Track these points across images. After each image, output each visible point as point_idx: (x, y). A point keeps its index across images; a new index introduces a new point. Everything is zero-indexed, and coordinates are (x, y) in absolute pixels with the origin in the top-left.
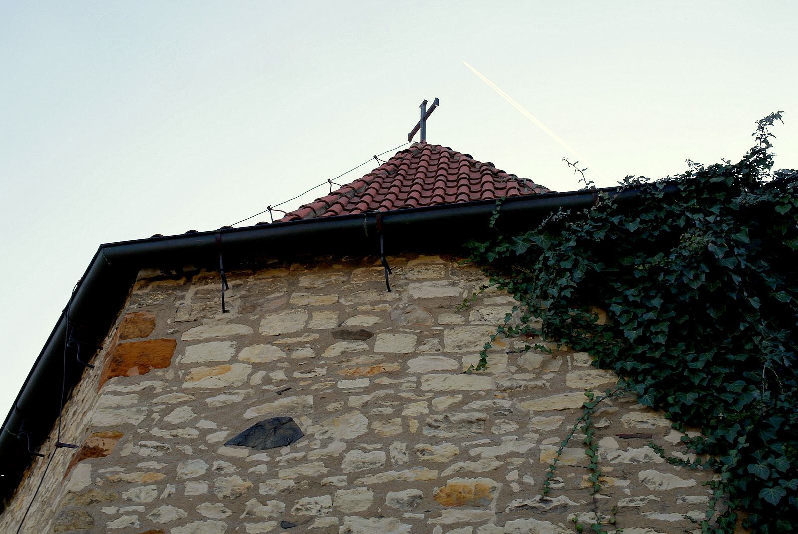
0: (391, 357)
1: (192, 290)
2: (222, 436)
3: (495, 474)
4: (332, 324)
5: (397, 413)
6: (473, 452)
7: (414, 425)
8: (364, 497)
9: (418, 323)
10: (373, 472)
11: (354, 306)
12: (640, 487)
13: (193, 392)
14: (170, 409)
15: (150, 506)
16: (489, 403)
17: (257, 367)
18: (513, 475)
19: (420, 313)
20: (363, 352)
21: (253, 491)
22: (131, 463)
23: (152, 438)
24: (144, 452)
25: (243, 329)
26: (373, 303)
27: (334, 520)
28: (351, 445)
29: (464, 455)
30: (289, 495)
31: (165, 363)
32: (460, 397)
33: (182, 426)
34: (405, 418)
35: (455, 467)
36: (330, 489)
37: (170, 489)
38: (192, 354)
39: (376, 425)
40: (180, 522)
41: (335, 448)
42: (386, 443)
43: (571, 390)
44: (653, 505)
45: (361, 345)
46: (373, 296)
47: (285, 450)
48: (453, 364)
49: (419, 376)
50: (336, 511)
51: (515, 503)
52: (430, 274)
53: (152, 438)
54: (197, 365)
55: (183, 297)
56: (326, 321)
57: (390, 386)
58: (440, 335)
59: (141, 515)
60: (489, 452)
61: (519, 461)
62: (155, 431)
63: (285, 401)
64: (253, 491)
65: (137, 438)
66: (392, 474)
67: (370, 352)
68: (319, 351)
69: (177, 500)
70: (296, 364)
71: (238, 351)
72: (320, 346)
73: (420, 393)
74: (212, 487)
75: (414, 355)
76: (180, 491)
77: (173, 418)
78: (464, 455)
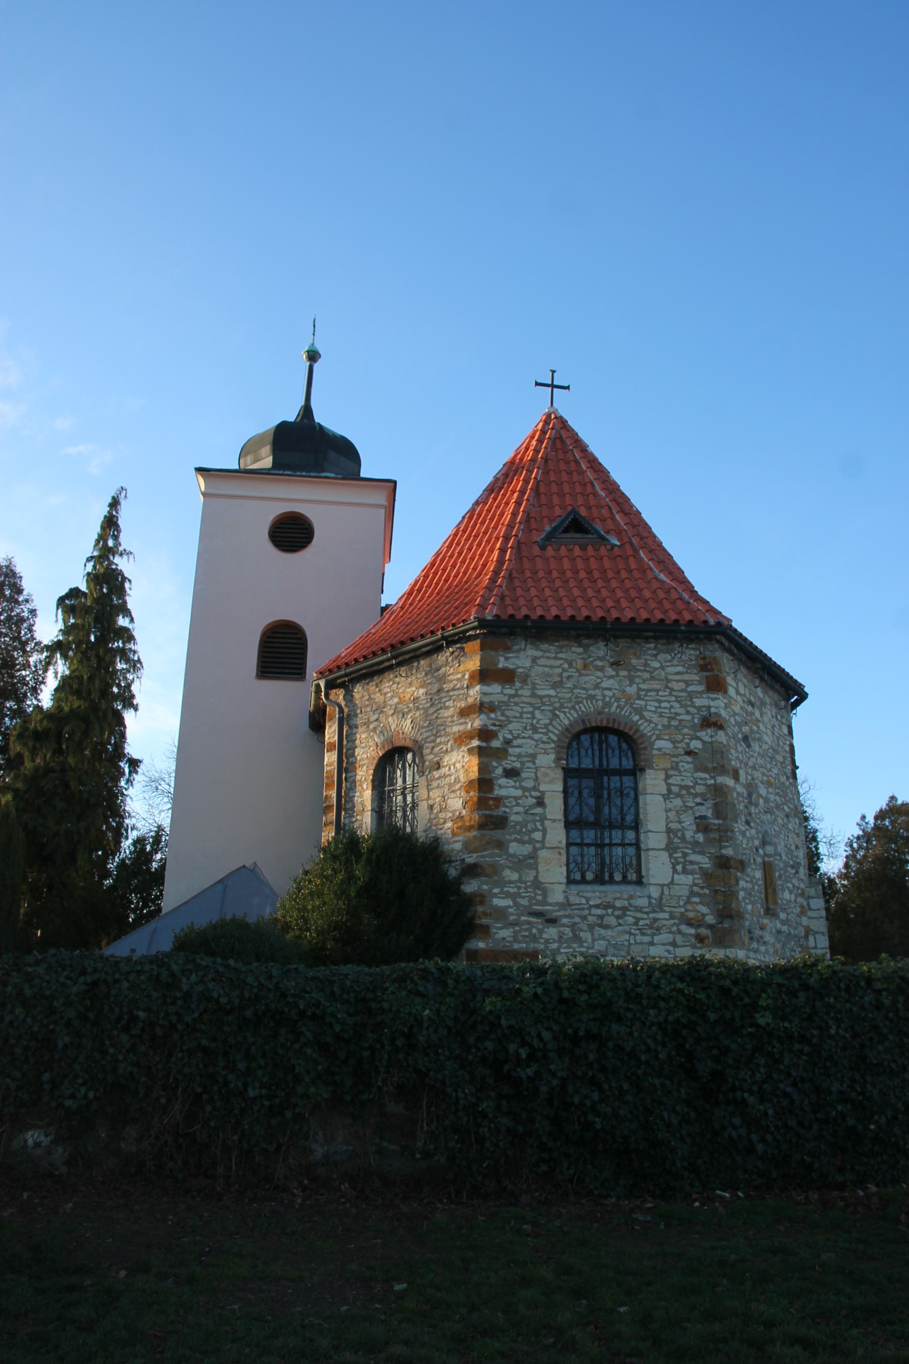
3: (774, 778)
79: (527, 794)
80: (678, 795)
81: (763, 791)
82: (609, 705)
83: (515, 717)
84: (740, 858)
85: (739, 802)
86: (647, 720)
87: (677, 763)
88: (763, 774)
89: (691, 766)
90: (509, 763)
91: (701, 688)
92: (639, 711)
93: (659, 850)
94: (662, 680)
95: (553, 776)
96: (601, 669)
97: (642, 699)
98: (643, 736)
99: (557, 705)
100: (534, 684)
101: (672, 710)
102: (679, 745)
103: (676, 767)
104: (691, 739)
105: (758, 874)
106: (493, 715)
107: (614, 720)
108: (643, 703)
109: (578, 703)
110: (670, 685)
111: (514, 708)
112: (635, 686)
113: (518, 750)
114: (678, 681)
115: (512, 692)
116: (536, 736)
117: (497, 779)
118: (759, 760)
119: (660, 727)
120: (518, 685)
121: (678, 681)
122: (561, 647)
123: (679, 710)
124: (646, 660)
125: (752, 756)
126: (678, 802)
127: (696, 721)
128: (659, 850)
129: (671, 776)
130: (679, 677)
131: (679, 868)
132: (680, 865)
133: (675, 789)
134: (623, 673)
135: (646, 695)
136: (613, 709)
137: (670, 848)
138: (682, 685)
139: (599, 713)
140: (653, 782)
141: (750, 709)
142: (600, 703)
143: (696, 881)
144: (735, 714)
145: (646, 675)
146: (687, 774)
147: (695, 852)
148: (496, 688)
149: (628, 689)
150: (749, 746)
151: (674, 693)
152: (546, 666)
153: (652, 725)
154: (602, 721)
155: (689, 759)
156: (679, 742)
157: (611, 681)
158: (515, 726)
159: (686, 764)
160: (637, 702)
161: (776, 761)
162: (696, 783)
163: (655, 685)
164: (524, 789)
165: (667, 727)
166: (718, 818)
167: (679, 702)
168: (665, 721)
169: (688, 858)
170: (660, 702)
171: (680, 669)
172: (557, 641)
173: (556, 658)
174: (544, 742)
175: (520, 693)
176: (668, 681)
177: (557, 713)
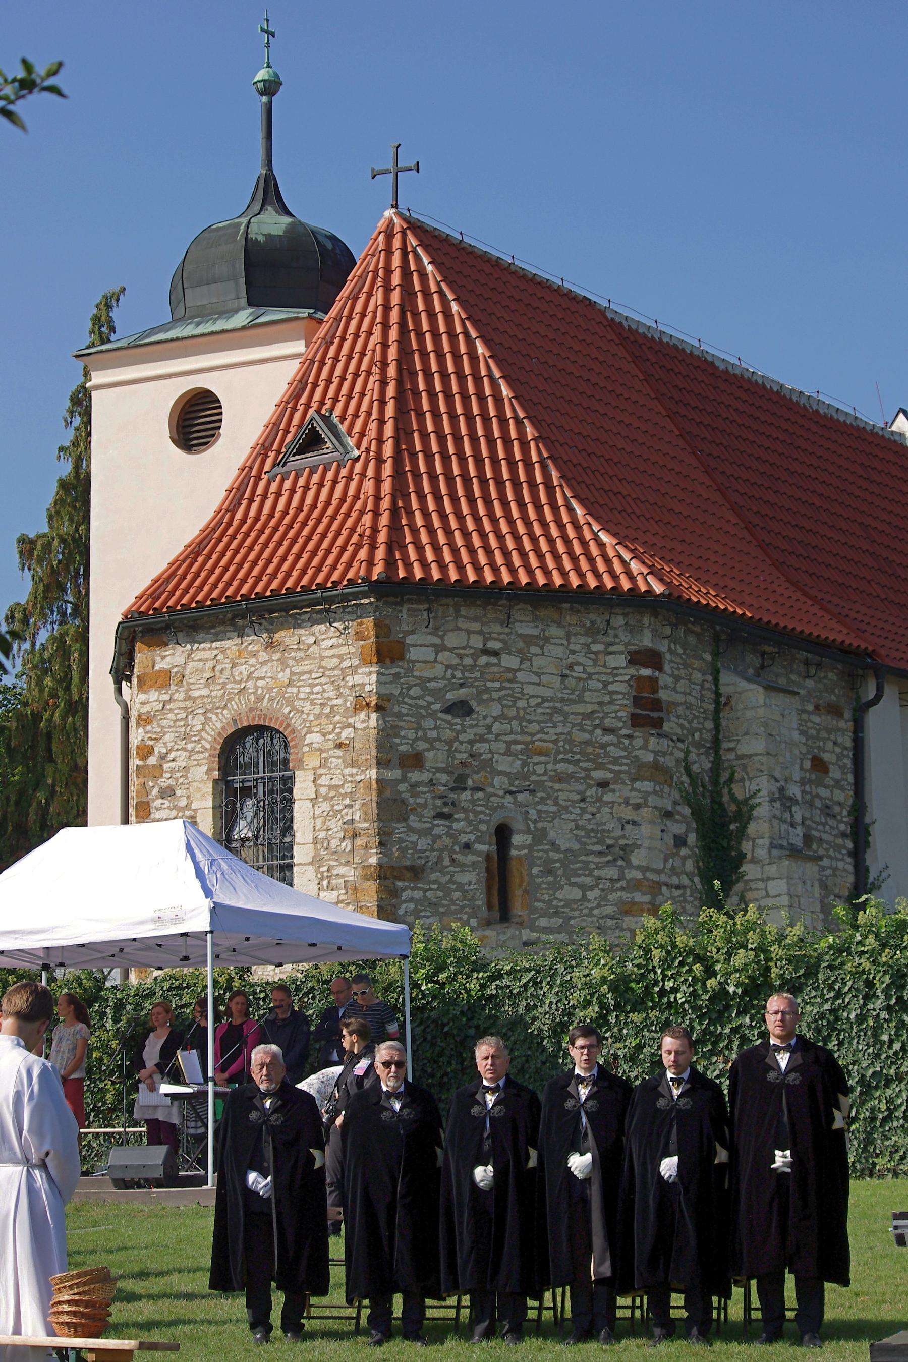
0: (509, 670)
1: (406, 607)
2: (437, 707)
3: (555, 742)
4: (481, 646)
5: (514, 705)
6: (546, 730)
7: (522, 713)
8: (502, 747)
9: (519, 651)
10: (506, 734)
11: (489, 633)
12: (607, 754)
13: (420, 678)
14: (409, 689)
15: (414, 741)
16: (551, 704)
17: (448, 667)
18: (561, 744)
19: (521, 645)
20: (495, 665)
21: (456, 739)
22: (399, 716)
23: (405, 703)
24: (404, 711)
25: (437, 641)
26: (499, 634)
27: (490, 756)
28: (496, 719)
29: (541, 731)
30: (471, 742)
31: (402, 658)
32: (540, 700)
33: (418, 698)
34: (518, 709)
35: (538, 736)
36: (488, 741)
37: (420, 733)
38: (414, 654)
39: (505, 710)
40: (428, 750)
41: (489, 720)
42: (511, 720)
43: (586, 702)
44: (609, 763)
45: (494, 660)
46: (497, 628)
47: (468, 719)
48: (535, 679)
49: (522, 683)
50: (491, 752)
51: (561, 756)
52: (527, 619)
53: (405, 703)
54: (418, 662)
55: (401, 611)
56: (477, 642)
57: (510, 688)
58: (530, 660)
59: (411, 745)
60: (552, 731)
61: (563, 737)
62: (406, 700)
63: (463, 691)
64: (456, 739)
65: (399, 703)
66: (512, 737)
67: (498, 665)
68: (475, 661)
69: (425, 739)
70: (465, 668)
71: (437, 655)
72: (475, 657)
73: (523, 694)
74: (438, 734)
75: (519, 670)
76: (425, 735)
77: (412, 692)
78: (541, 731)
79: (180, 814)
80: (326, 798)
81: (504, 764)
82: (260, 699)
83: (170, 727)
84: (408, 863)
85: (416, 795)
86: (298, 711)
87: (326, 759)
88: (516, 742)
89: (340, 761)
90: (165, 781)
91: (356, 662)
92: (290, 702)
93: (305, 864)
94: (315, 658)
95: (205, 790)
96: (254, 655)
97: (295, 686)
98: (293, 731)
99: (209, 707)
100: (189, 684)
101: (326, 695)
102: (331, 737)
103: (324, 764)
104: (342, 728)
105: (471, 879)
106: (149, 728)
107: (265, 715)
108: (295, 690)
109: (230, 700)
110: (324, 664)
111: (170, 716)
112: (288, 671)
113: (172, 765)
114: (332, 657)
115: (166, 697)
116: (190, 746)
117: (154, 800)
118: (496, 727)
119: (312, 718)
120: (173, 687)
121: (332, 657)
122: (216, 634)
123: (332, 694)
124: (300, 636)
125: (471, 727)
126: (325, 806)
127: (348, 704)
128: (305, 864)
129: (321, 775)
130: (331, 652)
131: (325, 883)
132: (325, 880)
133: (323, 791)
134: (276, 656)
135: (298, 681)
136: (266, 701)
137: (317, 861)
138: (335, 661)
139: (251, 710)
140: (302, 788)
141: (483, 660)
142: (252, 698)
143: (341, 898)
144: (423, 682)
145: (302, 654)
146: (338, 772)
147: (341, 864)
148: (153, 695)
149: (280, 675)
150: (469, 712)
151: (327, 673)
152: (200, 660)
153: (304, 716)
154: (254, 718)
155: (339, 752)
156: (330, 733)
157: (265, 668)
158: (169, 738)
159: (336, 759)
160: (289, 690)
161: (566, 716)
162: (345, 782)
163: (306, 666)
164: (182, 809)
165: (318, 717)
166: (365, 820)
167: (332, 683)
168: (317, 711)
169: (335, 872)
170: (312, 686)
171: (333, 641)
172: (214, 627)
173: (210, 649)
174: (198, 752)
175: (176, 696)
176: (322, 658)
177: (209, 715)
